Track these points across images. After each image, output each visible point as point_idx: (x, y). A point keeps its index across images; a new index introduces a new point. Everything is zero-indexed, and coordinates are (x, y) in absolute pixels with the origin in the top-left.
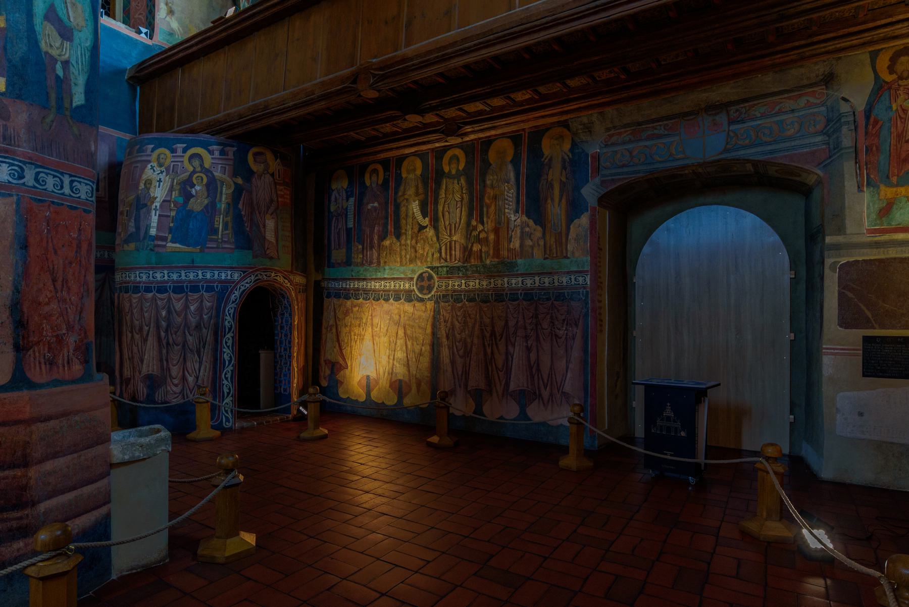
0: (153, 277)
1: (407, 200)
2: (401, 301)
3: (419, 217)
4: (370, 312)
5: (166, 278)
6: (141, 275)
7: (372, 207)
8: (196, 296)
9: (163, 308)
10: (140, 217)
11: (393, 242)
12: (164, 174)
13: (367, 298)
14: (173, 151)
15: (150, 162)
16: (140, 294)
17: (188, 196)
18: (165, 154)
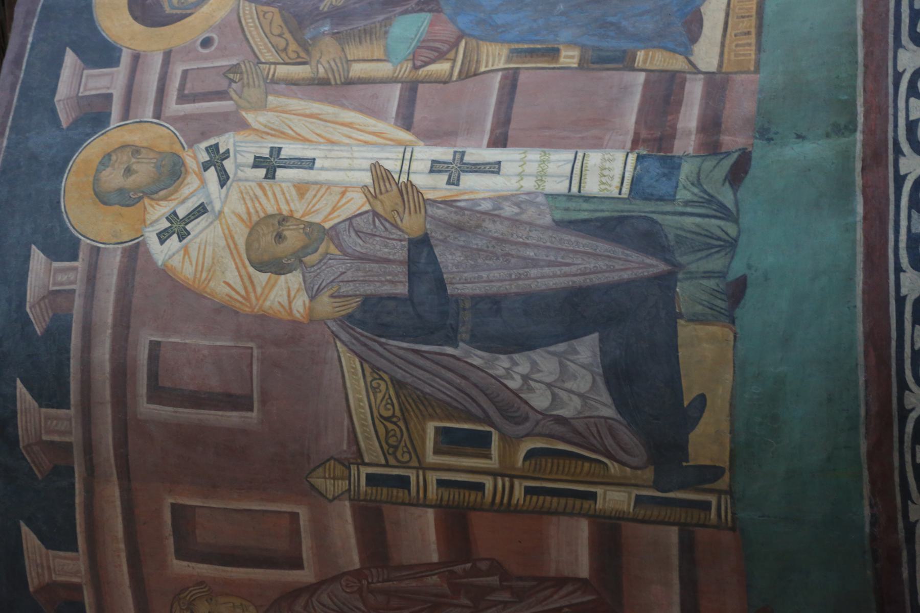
12: (226, 141)
18: (106, 160)
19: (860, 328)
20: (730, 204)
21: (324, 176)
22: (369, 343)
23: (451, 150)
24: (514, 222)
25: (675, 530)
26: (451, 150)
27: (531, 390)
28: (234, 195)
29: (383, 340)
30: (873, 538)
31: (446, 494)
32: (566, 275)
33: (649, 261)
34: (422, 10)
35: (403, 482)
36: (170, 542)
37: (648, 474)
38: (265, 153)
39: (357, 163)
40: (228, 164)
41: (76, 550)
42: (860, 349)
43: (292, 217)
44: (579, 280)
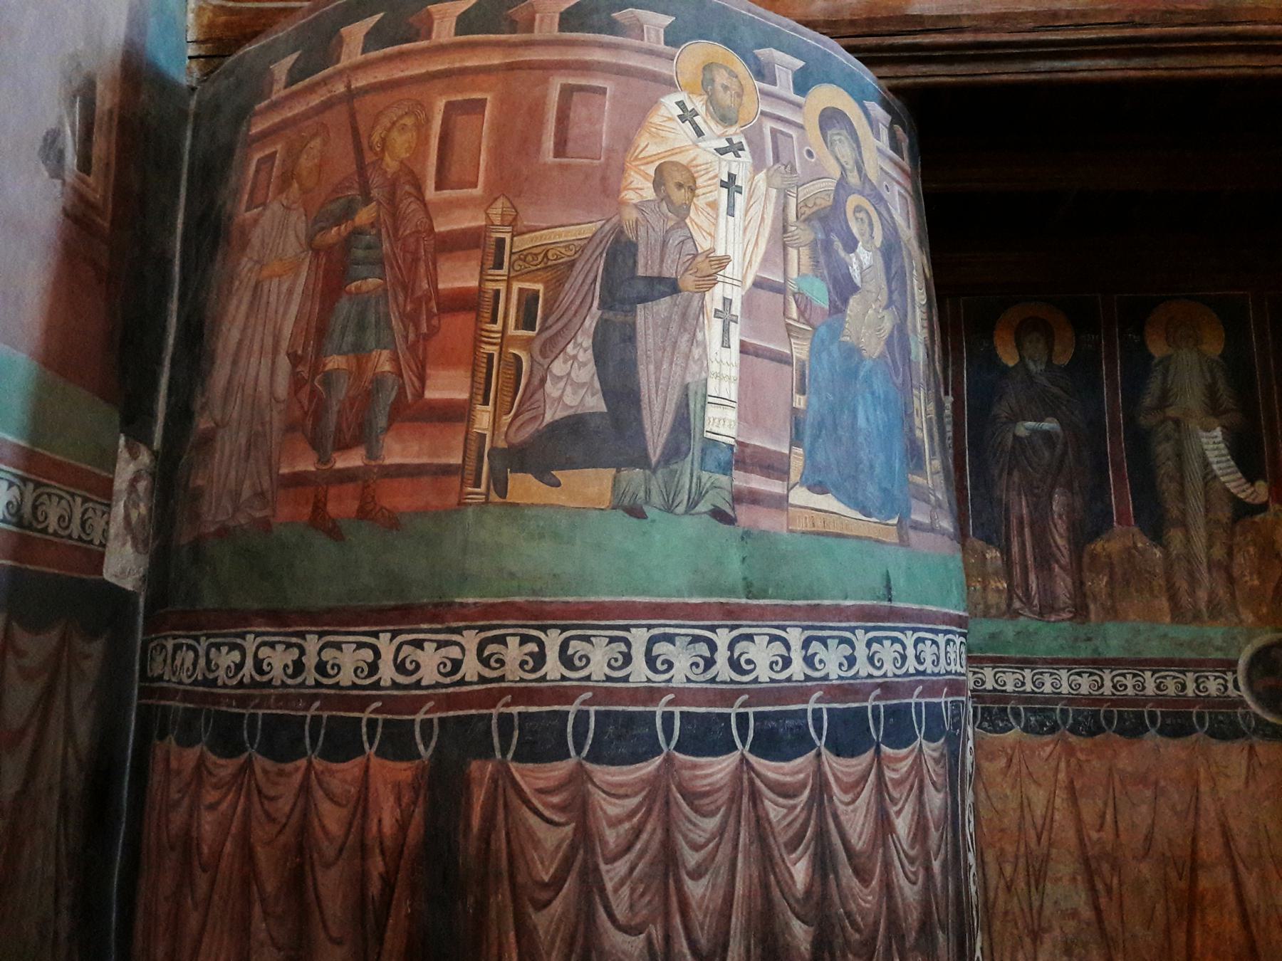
0: (734, 664)
1: (1177, 422)
2: (1194, 737)
3: (1233, 481)
4: (1062, 776)
5: (798, 669)
6: (661, 648)
7: (1034, 431)
8: (900, 761)
9: (793, 845)
10: (630, 338)
11: (1135, 547)
12: (746, 156)
13: (1042, 725)
14: (762, 72)
15: (670, 84)
16: (658, 760)
17: (843, 288)
18: (733, 75)
19: (607, 599)
20: (698, 509)
21: (722, 221)
22: (602, 245)
23: (738, 314)
24: (687, 356)
25: (460, 461)
26: (738, 314)
27: (565, 362)
28: (710, 158)
29: (604, 255)
30: (451, 604)
31: (490, 295)
32: (649, 390)
33: (658, 452)
34: (830, 302)
35: (499, 265)
36: (459, 98)
37: (502, 444)
38: (738, 182)
39: (730, 246)
40: (730, 156)
41: (456, 34)
42: (593, 599)
43: (694, 196)
44: (645, 399)
